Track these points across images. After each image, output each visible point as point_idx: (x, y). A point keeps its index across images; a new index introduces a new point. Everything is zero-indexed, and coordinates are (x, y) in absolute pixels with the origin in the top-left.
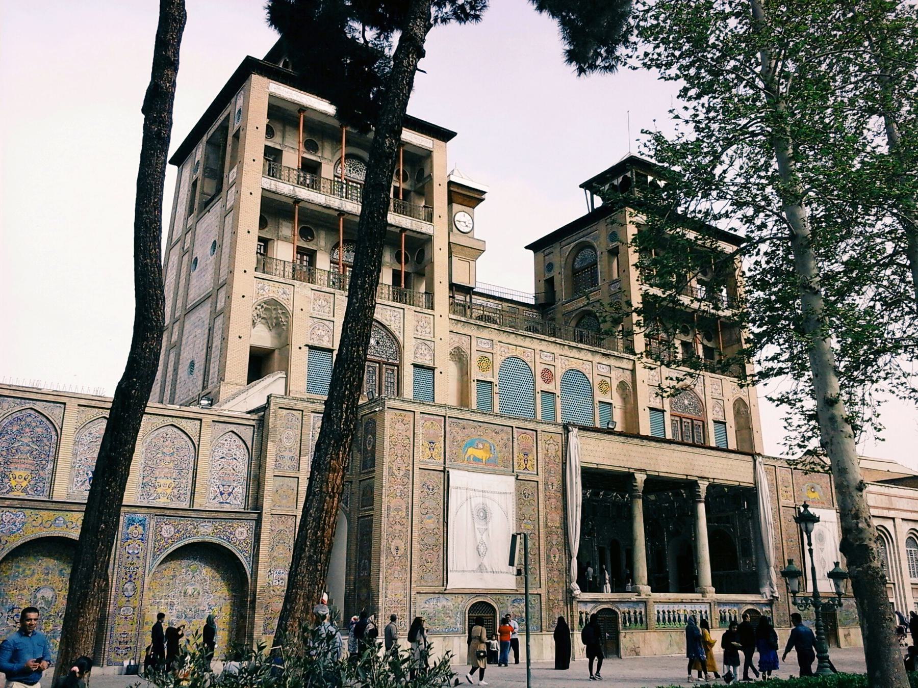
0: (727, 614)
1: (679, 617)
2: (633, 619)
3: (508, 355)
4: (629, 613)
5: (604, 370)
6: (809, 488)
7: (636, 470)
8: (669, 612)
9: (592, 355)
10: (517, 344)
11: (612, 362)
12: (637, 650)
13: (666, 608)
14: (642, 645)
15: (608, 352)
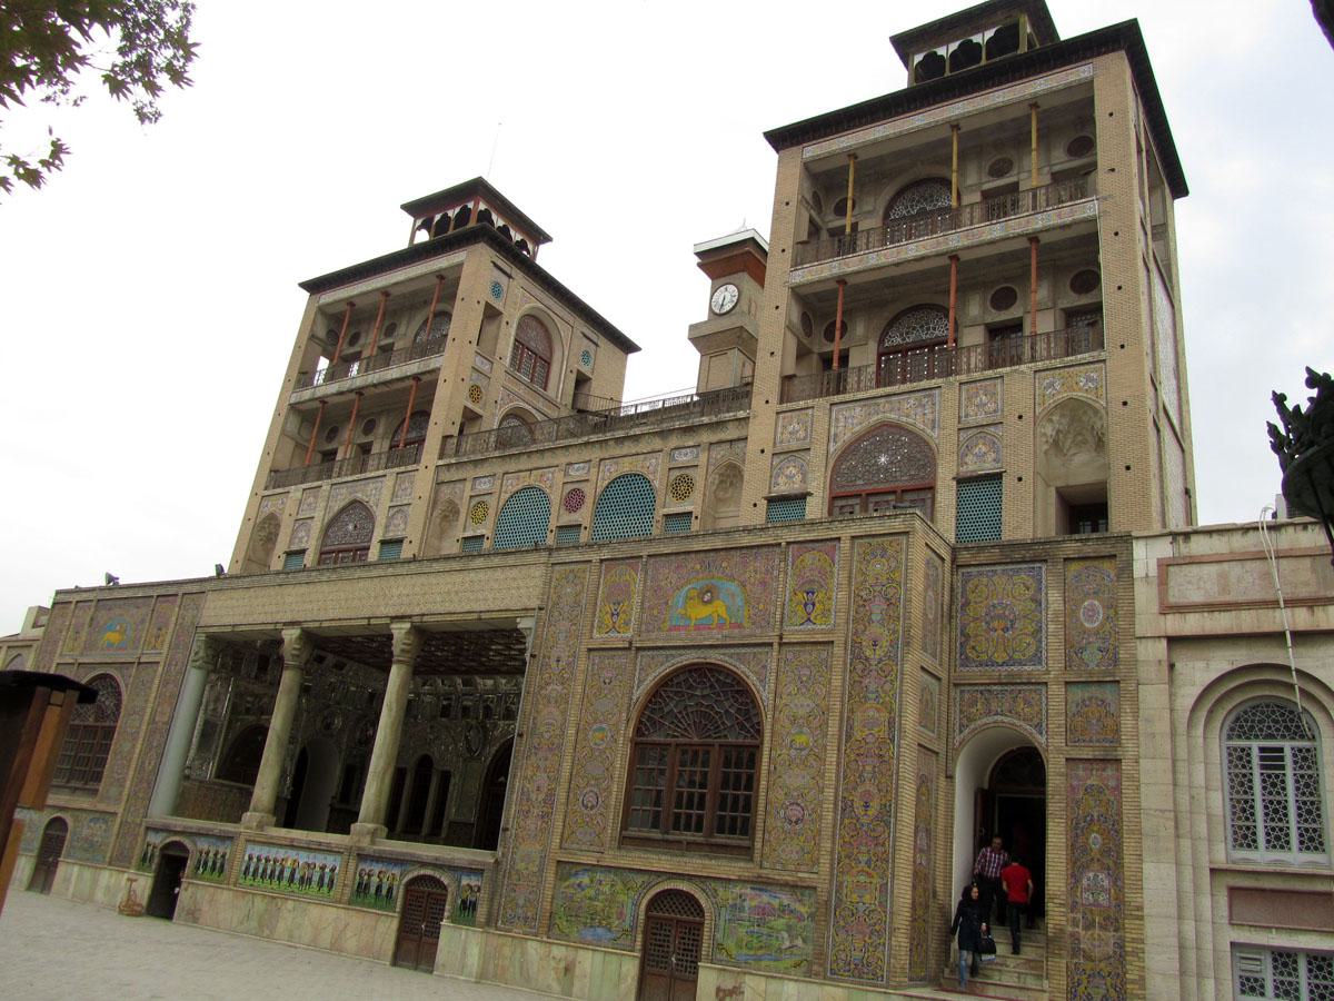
0: (375, 879)
1: (282, 872)
2: (210, 864)
3: (515, 489)
4: (207, 853)
5: (683, 458)
6: (694, 593)
7: (285, 624)
8: (267, 860)
9: (662, 439)
10: (530, 467)
11: (706, 437)
12: (197, 915)
13: (264, 852)
14: (205, 908)
15: (690, 422)
